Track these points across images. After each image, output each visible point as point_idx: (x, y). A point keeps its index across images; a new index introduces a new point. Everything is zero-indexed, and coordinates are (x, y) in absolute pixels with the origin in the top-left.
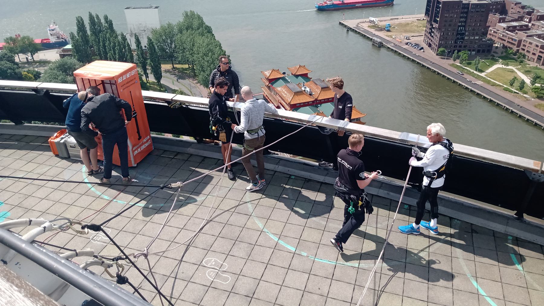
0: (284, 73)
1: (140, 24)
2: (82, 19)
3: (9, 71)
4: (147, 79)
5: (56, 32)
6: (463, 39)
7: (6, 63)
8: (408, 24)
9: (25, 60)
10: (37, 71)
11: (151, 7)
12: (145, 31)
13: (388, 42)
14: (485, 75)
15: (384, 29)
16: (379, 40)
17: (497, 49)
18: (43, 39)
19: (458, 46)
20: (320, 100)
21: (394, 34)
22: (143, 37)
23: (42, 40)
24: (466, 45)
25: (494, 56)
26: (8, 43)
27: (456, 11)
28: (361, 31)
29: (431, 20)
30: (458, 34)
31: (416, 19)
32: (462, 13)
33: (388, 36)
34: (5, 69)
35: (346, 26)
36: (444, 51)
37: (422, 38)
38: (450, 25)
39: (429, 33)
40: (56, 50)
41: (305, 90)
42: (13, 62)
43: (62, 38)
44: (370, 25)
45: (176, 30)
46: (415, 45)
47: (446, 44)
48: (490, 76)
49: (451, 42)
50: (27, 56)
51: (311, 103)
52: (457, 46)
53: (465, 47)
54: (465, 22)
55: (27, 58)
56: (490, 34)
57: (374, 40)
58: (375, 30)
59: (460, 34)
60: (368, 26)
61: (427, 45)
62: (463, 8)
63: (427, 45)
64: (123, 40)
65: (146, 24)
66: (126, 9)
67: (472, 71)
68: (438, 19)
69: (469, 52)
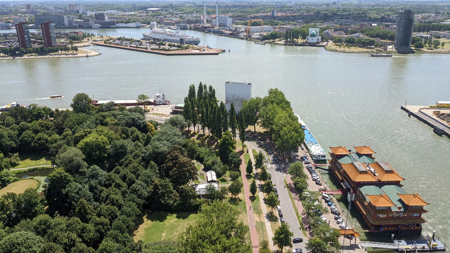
0: (350, 151)
2: (194, 87)
12: (237, 100)
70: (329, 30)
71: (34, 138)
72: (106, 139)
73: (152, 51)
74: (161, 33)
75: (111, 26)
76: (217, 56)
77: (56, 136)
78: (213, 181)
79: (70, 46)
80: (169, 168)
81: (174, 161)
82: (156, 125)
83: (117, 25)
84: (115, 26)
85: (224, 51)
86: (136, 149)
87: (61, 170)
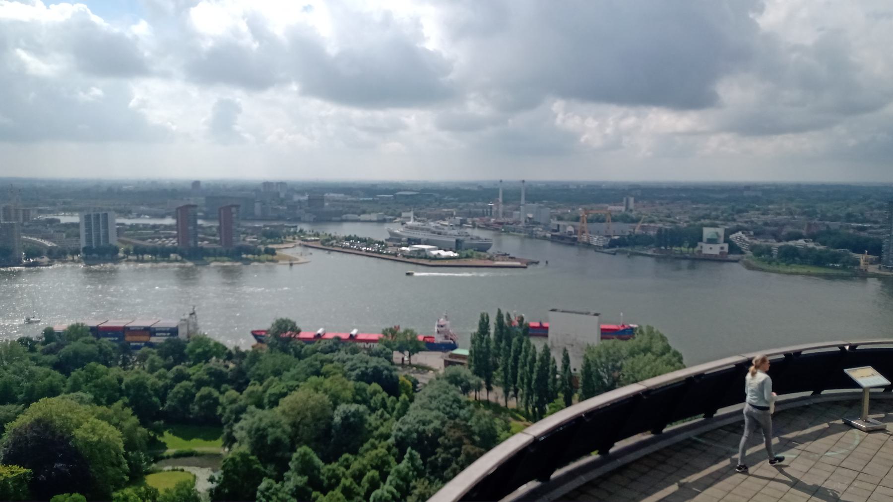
2: (488, 317)
3: (386, 372)
9: (400, 361)
11: (588, 313)
18: (426, 336)
23: (425, 337)
34: (382, 368)
40: (440, 354)
70: (743, 233)
71: (194, 396)
72: (326, 398)
73: (403, 259)
74: (422, 229)
75: (334, 218)
77: (232, 393)
79: (262, 248)
81: (453, 450)
83: (344, 217)
84: (338, 219)
85: (537, 263)
86: (382, 424)
87: (245, 448)
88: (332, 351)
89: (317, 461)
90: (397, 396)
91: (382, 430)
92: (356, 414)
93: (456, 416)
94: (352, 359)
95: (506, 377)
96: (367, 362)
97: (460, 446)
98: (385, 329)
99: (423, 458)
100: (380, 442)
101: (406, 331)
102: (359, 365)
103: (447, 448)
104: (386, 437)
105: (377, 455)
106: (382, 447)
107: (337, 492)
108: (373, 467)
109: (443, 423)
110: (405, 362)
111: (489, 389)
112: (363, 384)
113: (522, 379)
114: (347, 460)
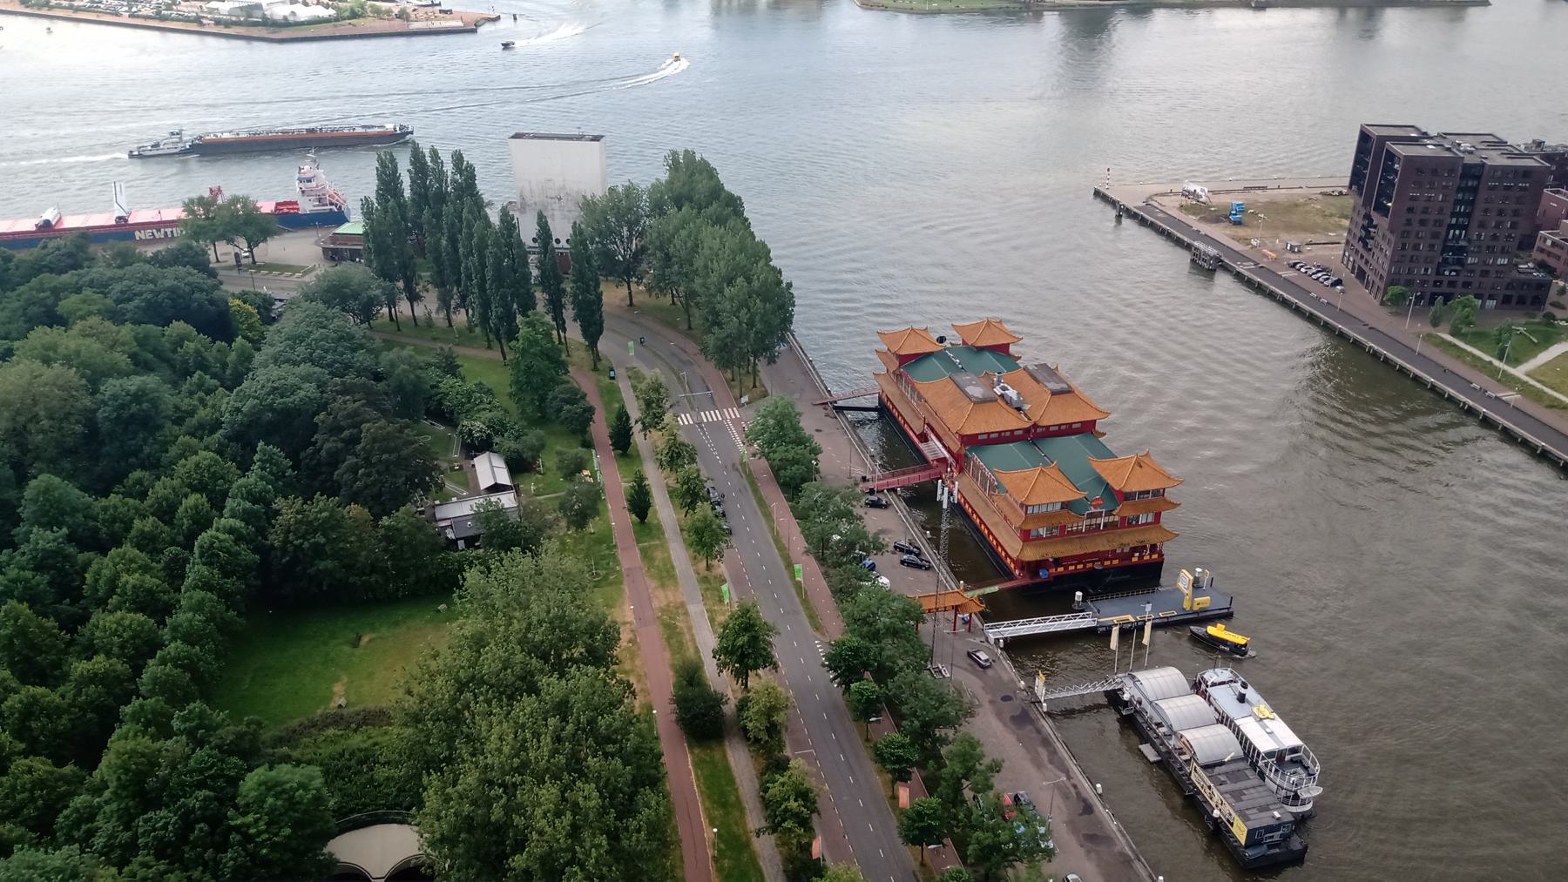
1: (550, 180)
3: (197, 295)
4: (562, 334)
5: (317, 186)
6: (1461, 263)
7: (189, 273)
8: (1296, 205)
9: (233, 262)
10: (266, 295)
11: (580, 138)
12: (560, 199)
13: (1243, 258)
14: (1528, 374)
15: (1227, 217)
16: (1212, 251)
17: (1563, 297)
19: (1445, 283)
20: (1048, 427)
21: (1259, 233)
22: (553, 215)
23: (278, 204)
24: (1470, 280)
25: (1554, 318)
26: (191, 212)
27: (1444, 184)
28: (1157, 218)
29: (1366, 204)
30: (1445, 249)
31: (1319, 191)
32: (1459, 190)
33: (1239, 240)
34: (187, 289)
35: (1113, 203)
36: (1403, 296)
37: (1338, 251)
38: (1423, 223)
39: (1361, 239)
41: (1002, 396)
42: (202, 265)
43: (331, 204)
44: (1184, 203)
45: (645, 203)
46: (1318, 272)
47: (1409, 273)
48: (1542, 378)
49: (1426, 270)
50: (237, 250)
51: (1021, 432)
52: (1441, 282)
53: (1466, 285)
54: (1468, 215)
55: (237, 255)
56: (1542, 250)
57: (1196, 249)
58: (1201, 219)
59: (1452, 249)
60: (1177, 205)
61: (1352, 272)
62: (1463, 176)
63: (1352, 272)
64: (506, 229)
65: (564, 180)
66: (513, 137)
67: (1487, 358)
68: (1390, 204)
69: (1479, 302)
76: (469, 38)
78: (497, 488)
80: (335, 460)
81: (346, 433)
82: (265, 304)
86: (202, 401)
88: (76, 266)
89: (75, 494)
90: (230, 341)
91: (203, 413)
92: (138, 397)
93: (348, 367)
94: (121, 279)
95: (440, 272)
96: (153, 281)
97: (357, 426)
98: (187, 201)
99: (293, 455)
100: (201, 439)
101: (235, 200)
102: (138, 288)
103: (336, 429)
104: (216, 425)
105: (197, 465)
106: (207, 448)
107: (128, 550)
108: (194, 489)
109: (321, 386)
110: (244, 261)
111: (414, 298)
112: (152, 328)
113: (469, 278)
114: (139, 482)
